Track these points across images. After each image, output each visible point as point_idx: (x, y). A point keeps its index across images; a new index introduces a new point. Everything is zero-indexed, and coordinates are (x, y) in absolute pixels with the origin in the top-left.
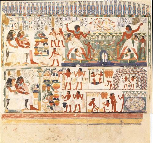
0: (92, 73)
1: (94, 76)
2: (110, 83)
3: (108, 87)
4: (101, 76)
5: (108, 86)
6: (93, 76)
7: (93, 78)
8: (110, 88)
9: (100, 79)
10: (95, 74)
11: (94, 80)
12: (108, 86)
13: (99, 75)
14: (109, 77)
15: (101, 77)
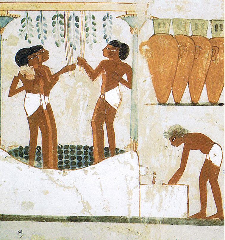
0: (23, 57)
1: (43, 82)
2: (196, 158)
3: (179, 190)
4: (109, 86)
5: (174, 180)
6: (31, 87)
7: (33, 102)
8: (196, 209)
9: (104, 114)
10: (54, 64)
11: (42, 120)
12: (174, 180)
13: (93, 75)
14: (186, 97)
15: (112, 97)
